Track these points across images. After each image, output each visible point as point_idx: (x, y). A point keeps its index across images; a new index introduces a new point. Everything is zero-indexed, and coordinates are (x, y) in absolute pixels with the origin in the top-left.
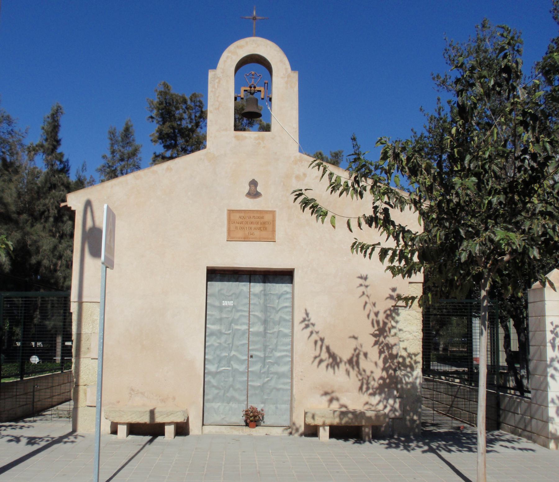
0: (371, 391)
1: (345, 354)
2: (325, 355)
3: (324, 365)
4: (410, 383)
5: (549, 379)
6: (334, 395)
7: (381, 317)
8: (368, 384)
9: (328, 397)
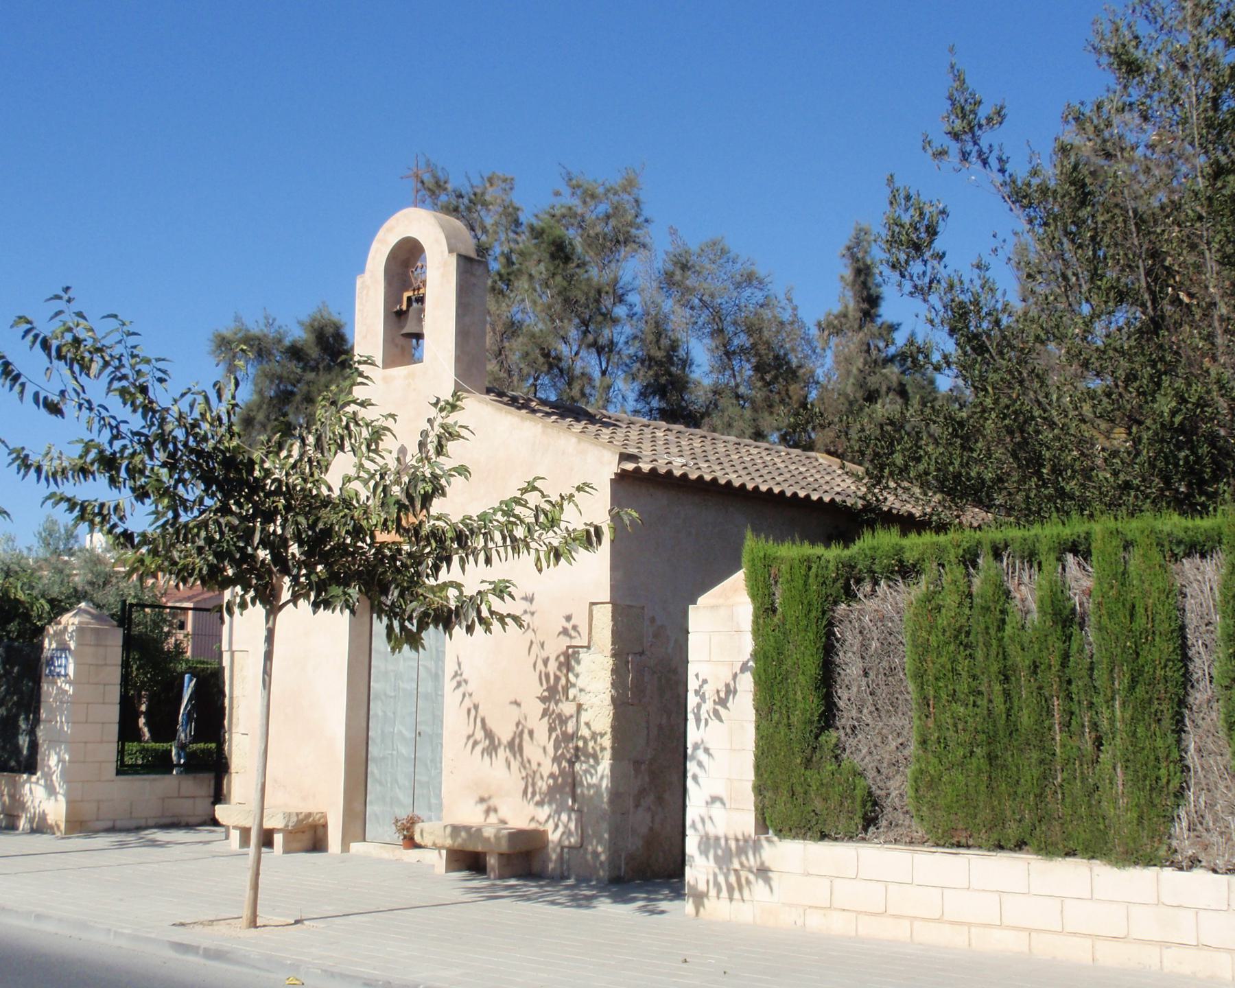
0: (537, 798)
1: (505, 733)
2: (480, 734)
3: (479, 748)
4: (594, 785)
5: (690, 782)
6: (492, 803)
7: (552, 667)
8: (534, 785)
9: (484, 807)
